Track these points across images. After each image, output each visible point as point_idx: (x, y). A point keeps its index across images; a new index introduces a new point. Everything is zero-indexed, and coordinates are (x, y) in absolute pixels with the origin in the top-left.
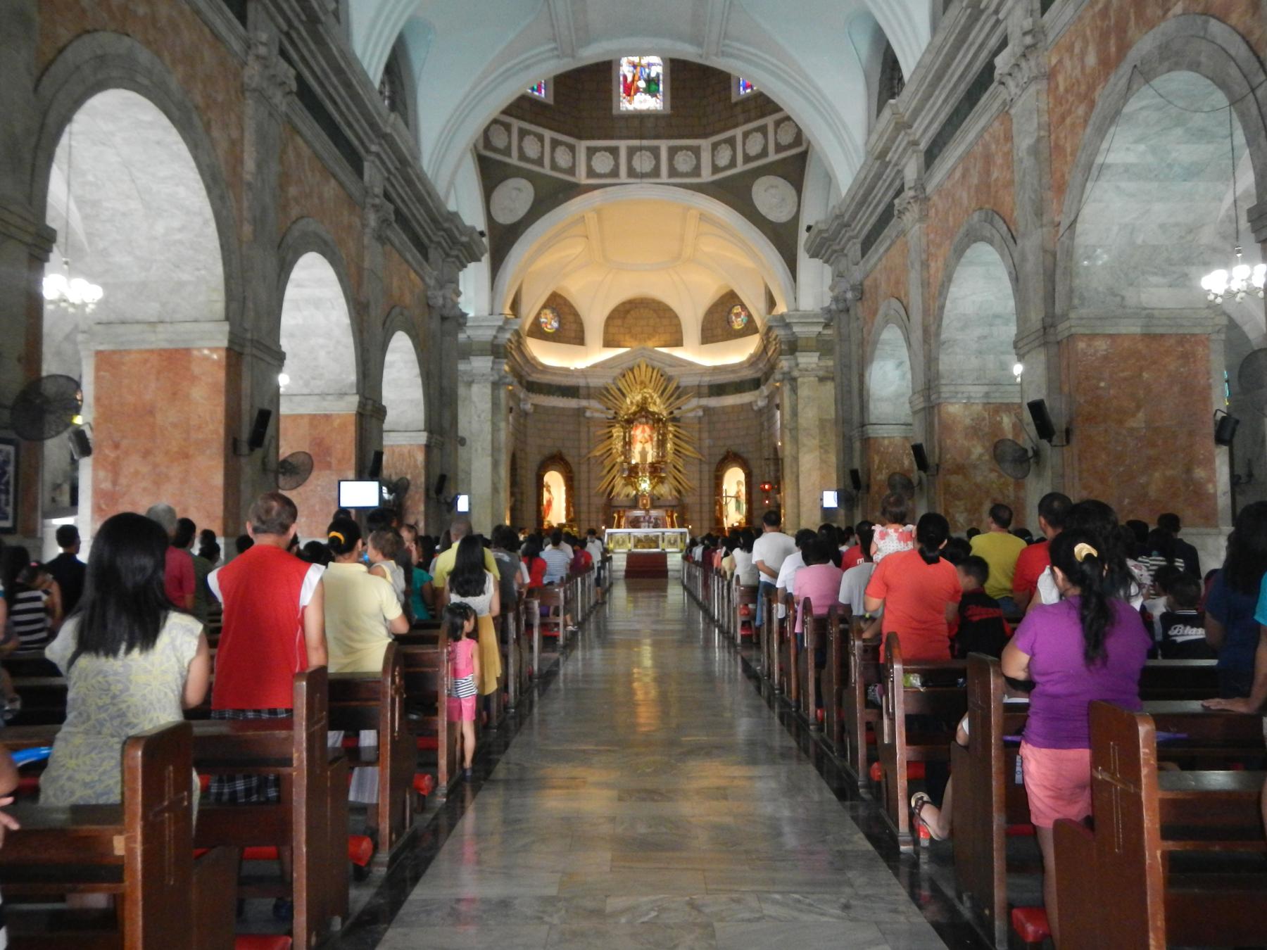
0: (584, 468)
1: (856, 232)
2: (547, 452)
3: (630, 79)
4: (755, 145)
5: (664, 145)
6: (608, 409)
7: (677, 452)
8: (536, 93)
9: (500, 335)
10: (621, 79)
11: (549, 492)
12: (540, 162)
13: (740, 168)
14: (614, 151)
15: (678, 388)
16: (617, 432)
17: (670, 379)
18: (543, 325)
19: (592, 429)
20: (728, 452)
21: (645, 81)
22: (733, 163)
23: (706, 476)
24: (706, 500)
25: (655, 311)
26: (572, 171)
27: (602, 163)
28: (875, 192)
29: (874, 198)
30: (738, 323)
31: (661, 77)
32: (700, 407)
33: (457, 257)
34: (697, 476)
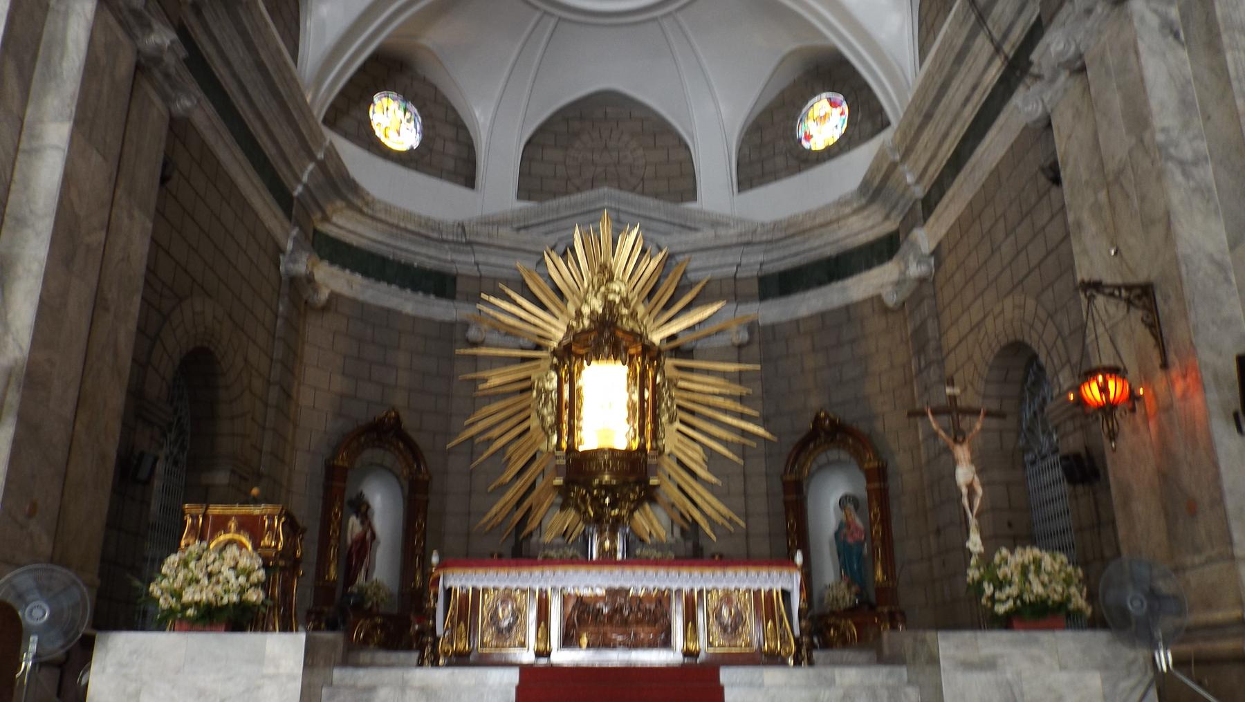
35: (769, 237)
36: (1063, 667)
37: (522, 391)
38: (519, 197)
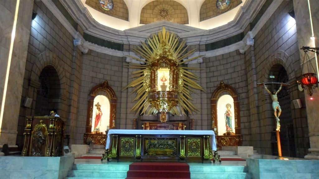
0: (124, 95)
2: (97, 82)
6: (141, 58)
7: (185, 86)
11: (99, 109)
15: (186, 46)
16: (146, 73)
17: (180, 41)
18: (102, 5)
19: (130, 70)
20: (221, 84)
23: (205, 101)
24: (205, 117)
25: (172, 6)
32: (200, 56)
34: (199, 101)
35: (209, 34)
36: (298, 172)
37: (141, 76)
38: (140, 23)
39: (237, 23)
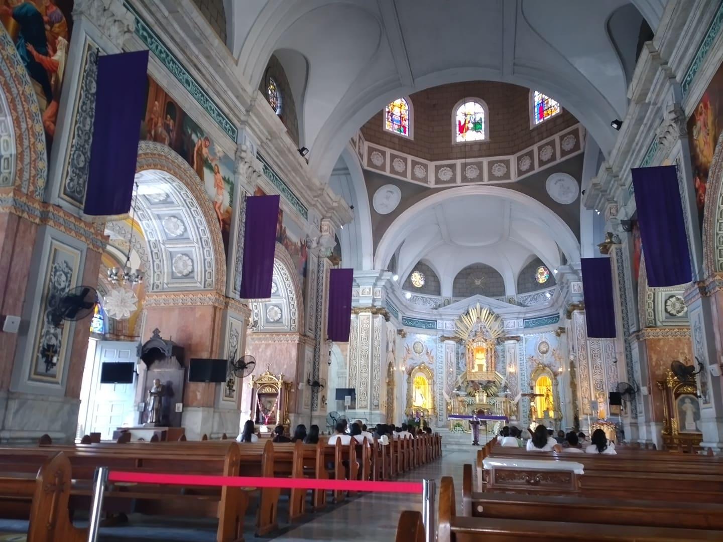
1: (623, 180)
3: (462, 123)
4: (547, 154)
5: (485, 161)
8: (403, 134)
9: (378, 283)
10: (457, 123)
12: (404, 174)
13: (537, 169)
14: (452, 167)
21: (473, 123)
22: (532, 167)
26: (425, 180)
27: (446, 175)
28: (637, 138)
29: (637, 144)
30: (542, 279)
31: (483, 120)
33: (331, 218)
39: (552, 306)
